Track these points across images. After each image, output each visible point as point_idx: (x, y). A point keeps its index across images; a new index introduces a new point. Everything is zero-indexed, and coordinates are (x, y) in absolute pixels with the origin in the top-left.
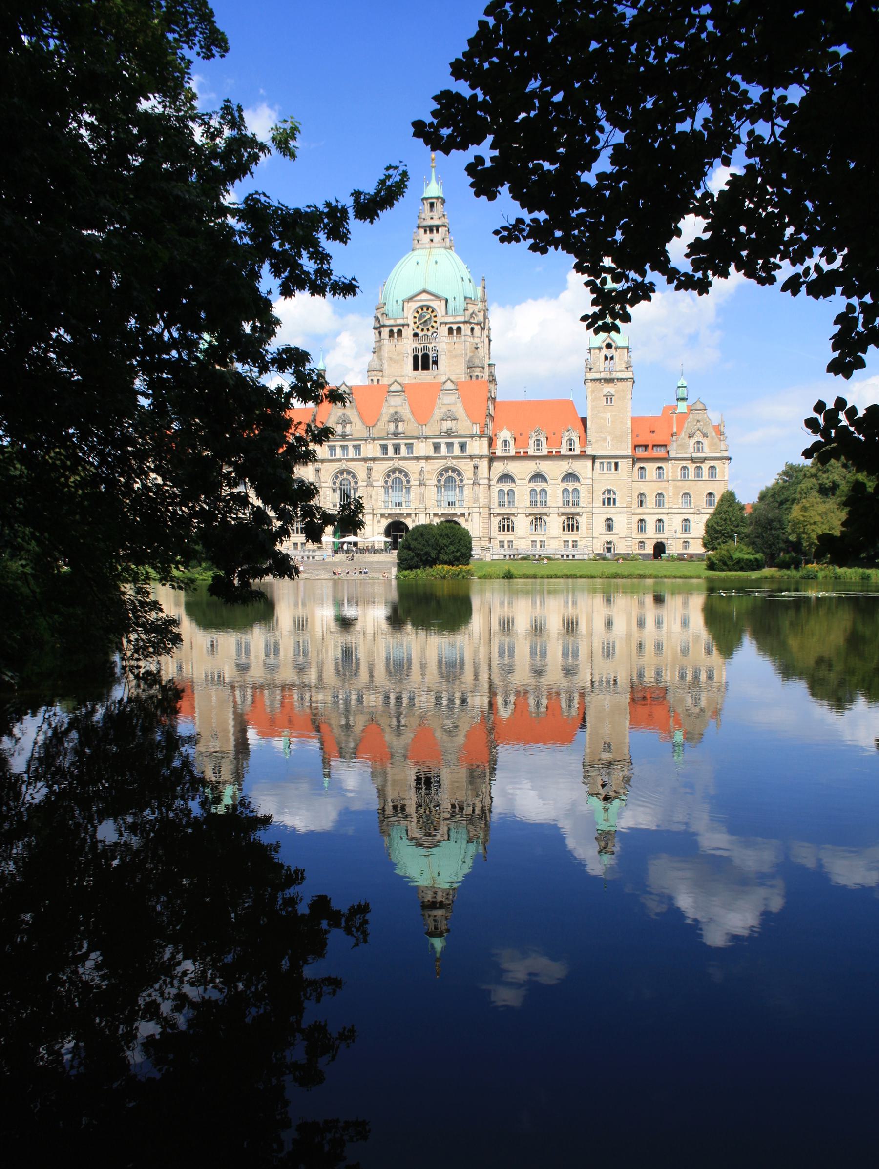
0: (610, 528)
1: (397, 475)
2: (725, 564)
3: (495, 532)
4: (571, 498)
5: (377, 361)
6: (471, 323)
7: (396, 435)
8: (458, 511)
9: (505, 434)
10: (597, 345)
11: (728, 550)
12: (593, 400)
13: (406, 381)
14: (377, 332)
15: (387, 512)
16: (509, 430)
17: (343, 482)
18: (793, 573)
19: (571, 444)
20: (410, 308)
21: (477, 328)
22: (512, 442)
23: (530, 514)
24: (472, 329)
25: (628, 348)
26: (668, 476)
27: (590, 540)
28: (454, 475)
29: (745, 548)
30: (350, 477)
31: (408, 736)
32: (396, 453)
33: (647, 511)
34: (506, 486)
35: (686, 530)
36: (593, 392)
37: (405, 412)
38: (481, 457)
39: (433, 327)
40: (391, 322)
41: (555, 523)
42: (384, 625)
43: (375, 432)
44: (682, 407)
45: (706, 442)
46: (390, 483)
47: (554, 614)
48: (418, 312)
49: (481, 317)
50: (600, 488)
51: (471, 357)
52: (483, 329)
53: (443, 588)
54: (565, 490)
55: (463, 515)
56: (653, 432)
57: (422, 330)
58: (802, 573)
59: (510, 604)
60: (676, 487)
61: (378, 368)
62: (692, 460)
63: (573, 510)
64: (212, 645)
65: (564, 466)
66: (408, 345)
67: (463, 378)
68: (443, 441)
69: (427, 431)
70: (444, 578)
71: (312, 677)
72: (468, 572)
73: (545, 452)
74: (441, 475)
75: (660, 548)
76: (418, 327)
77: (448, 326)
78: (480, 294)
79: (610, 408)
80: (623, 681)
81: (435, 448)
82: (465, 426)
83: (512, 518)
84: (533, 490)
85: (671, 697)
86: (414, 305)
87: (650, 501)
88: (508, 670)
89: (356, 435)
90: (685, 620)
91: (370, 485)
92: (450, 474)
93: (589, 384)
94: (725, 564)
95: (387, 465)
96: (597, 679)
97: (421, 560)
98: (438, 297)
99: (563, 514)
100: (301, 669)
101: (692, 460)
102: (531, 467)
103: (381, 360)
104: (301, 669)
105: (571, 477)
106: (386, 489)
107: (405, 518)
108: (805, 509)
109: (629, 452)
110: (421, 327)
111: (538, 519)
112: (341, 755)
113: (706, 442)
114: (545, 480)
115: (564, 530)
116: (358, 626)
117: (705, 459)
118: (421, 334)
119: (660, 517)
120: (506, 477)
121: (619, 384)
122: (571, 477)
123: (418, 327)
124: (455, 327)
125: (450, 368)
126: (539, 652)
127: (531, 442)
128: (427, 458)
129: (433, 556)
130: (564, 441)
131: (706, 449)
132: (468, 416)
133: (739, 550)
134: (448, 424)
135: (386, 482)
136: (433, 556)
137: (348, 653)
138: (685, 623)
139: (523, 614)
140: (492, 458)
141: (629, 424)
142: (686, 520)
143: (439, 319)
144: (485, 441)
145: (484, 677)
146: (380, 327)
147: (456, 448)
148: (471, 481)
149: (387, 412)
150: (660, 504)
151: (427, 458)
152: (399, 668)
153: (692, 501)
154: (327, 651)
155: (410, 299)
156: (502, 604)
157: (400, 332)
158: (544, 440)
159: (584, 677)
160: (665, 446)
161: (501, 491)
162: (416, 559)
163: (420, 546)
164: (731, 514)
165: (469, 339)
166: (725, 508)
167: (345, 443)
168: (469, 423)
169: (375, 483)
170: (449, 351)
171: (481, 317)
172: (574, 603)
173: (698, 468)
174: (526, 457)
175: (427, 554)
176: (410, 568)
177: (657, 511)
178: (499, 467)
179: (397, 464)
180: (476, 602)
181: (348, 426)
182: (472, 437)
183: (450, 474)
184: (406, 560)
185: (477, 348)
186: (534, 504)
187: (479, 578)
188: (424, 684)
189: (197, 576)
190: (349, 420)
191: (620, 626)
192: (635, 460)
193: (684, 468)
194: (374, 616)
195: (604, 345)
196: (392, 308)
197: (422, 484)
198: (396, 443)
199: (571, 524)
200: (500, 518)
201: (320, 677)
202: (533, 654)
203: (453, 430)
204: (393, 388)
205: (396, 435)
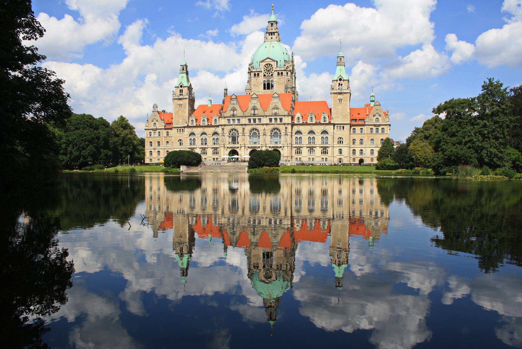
1: (255, 131)
2: (383, 167)
3: (294, 154)
4: (325, 140)
5: (249, 86)
7: (254, 115)
8: (279, 145)
9: (298, 115)
10: (336, 79)
11: (384, 162)
12: (334, 101)
13: (261, 93)
15: (250, 146)
16: (300, 113)
18: (410, 171)
21: (289, 73)
22: (301, 118)
23: (308, 147)
24: (287, 73)
25: (348, 80)
27: (333, 157)
28: (278, 131)
29: (391, 161)
30: (235, 132)
31: (258, 237)
34: (298, 136)
35: (370, 155)
36: (334, 98)
37: (258, 106)
38: (288, 124)
40: (255, 70)
41: (318, 151)
43: (246, 114)
44: (372, 104)
45: (380, 118)
47: (317, 188)
49: (291, 68)
50: (336, 137)
52: (292, 73)
53: (266, 177)
54: (322, 137)
55: (281, 147)
58: (413, 171)
59: (300, 184)
60: (368, 136)
62: (375, 125)
63: (325, 146)
65: (322, 128)
66: (261, 79)
67: (283, 92)
68: (273, 118)
69: (267, 113)
70: (267, 172)
71: (219, 212)
73: (314, 122)
74: (272, 131)
75: (361, 161)
78: (291, 59)
82: (282, 111)
84: (309, 137)
85: (366, 222)
86: (264, 64)
87: (358, 142)
88: (298, 211)
90: (370, 191)
92: (276, 131)
93: (333, 95)
94: (383, 167)
95: (250, 127)
96: (335, 214)
98: (274, 61)
99: (321, 147)
100: (215, 209)
101: (375, 125)
102: (308, 128)
104: (215, 209)
105: (325, 132)
106: (250, 137)
108: (415, 145)
111: (311, 149)
112: (231, 245)
113: (380, 118)
116: (239, 192)
117: (380, 125)
118: (267, 75)
119: (361, 149)
120: (299, 132)
122: (325, 132)
124: (280, 72)
125: (278, 88)
126: (311, 203)
127: (309, 118)
128: (267, 124)
130: (322, 118)
131: (380, 121)
132: (283, 107)
133: (389, 161)
135: (250, 134)
137: (234, 203)
138: (372, 192)
139: (305, 187)
140: (293, 125)
141: (349, 111)
142: (372, 150)
143: (274, 69)
144: (290, 118)
145: (289, 214)
147: (278, 120)
149: (251, 106)
150: (361, 143)
151: (267, 124)
152: (254, 209)
155: (263, 61)
156: (297, 184)
157: (258, 74)
158: (314, 117)
159: (329, 214)
160: (364, 120)
161: (296, 138)
166: (386, 145)
168: (283, 110)
171: (291, 68)
172: (326, 184)
174: (307, 124)
176: (253, 168)
178: (296, 128)
179: (254, 126)
180: (282, 182)
182: (285, 116)
183: (276, 131)
186: (310, 143)
187: (281, 172)
188: (264, 216)
191: (345, 193)
192: (351, 126)
193: (371, 129)
194: (245, 187)
196: (255, 65)
197: (265, 135)
198: (254, 118)
199: (325, 151)
200: (296, 149)
201: (223, 212)
202: (309, 204)
204: (253, 96)
205: (254, 115)
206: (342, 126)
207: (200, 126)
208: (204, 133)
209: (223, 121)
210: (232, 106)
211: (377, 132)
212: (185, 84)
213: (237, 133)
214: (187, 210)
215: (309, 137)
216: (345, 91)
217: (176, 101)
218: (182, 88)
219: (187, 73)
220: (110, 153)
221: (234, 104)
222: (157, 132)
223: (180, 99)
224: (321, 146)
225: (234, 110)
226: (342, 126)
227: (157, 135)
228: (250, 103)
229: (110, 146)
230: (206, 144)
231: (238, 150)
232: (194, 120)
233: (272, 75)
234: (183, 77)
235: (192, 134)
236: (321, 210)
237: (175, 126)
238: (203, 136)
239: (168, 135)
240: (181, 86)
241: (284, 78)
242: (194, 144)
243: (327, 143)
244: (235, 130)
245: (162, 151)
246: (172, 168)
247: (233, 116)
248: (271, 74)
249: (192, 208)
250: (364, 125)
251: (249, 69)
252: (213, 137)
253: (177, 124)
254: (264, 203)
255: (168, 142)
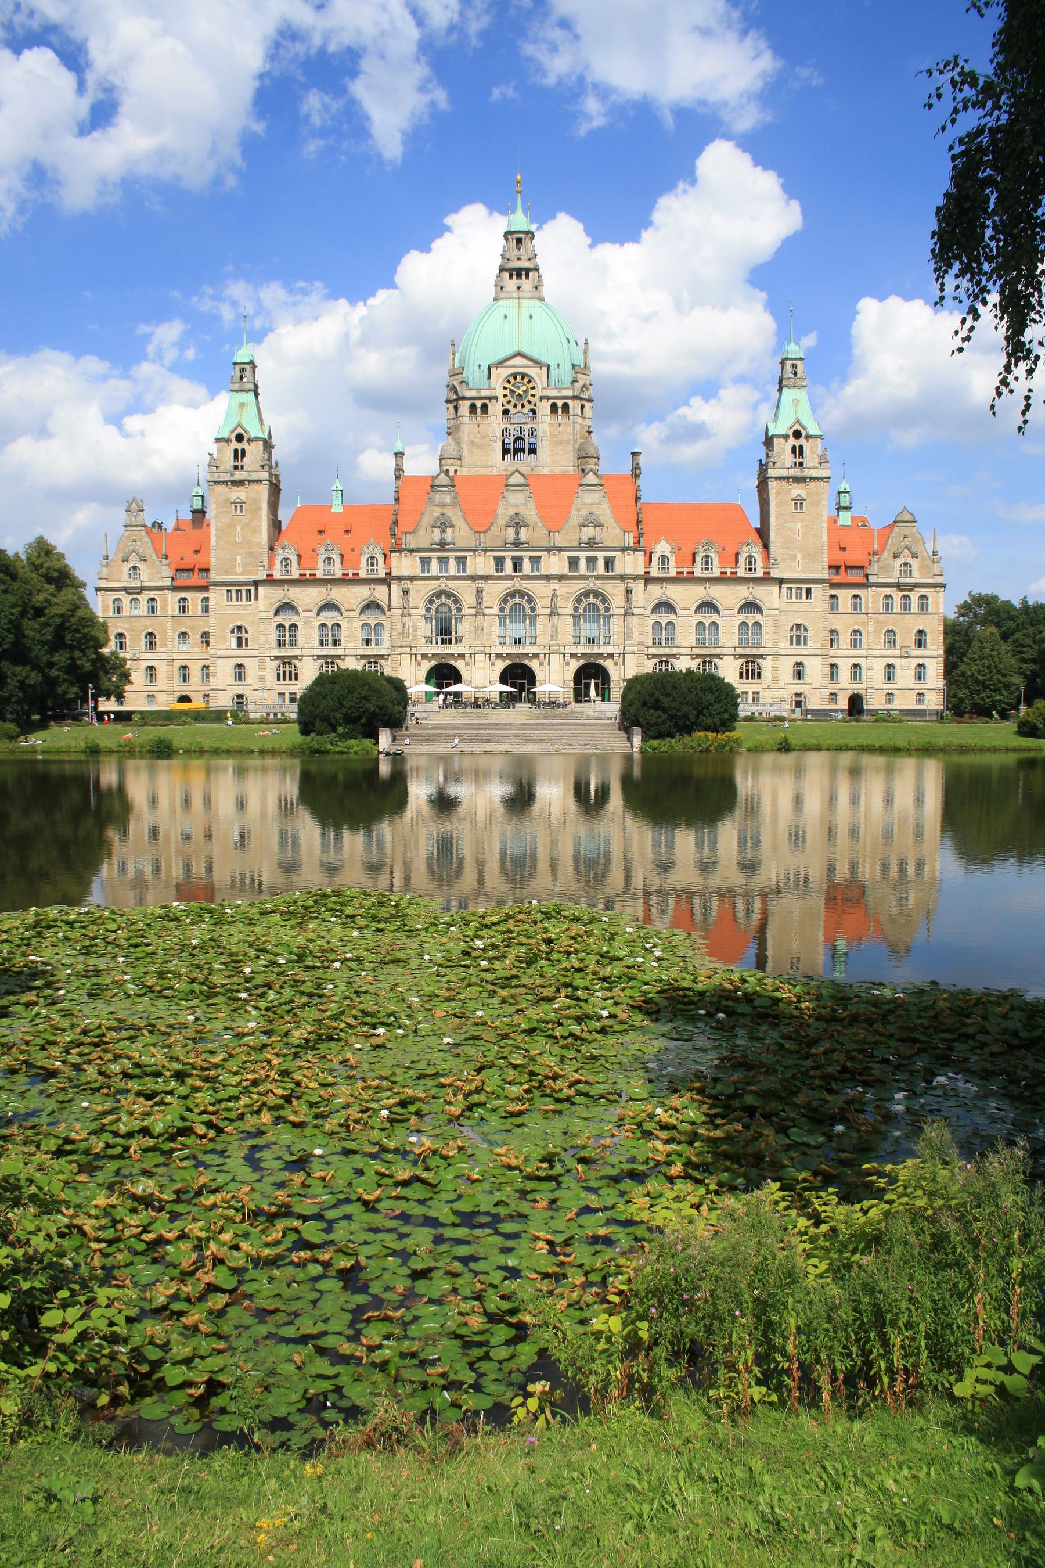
0: (799, 675)
1: (517, 600)
6: (581, 399)
7: (517, 544)
8: (605, 650)
9: (662, 548)
10: (783, 432)
12: (778, 506)
13: (495, 472)
14: (451, 406)
15: (505, 650)
17: (444, 609)
19: (750, 563)
20: (499, 376)
22: (672, 560)
24: (582, 407)
26: (866, 607)
28: (598, 602)
30: (450, 602)
32: (515, 570)
33: (840, 653)
36: (778, 494)
37: (530, 513)
38: (636, 578)
39: (529, 402)
42: (500, 810)
43: (486, 541)
46: (507, 611)
48: (509, 382)
51: (582, 444)
54: (744, 624)
56: (844, 549)
57: (515, 406)
60: (877, 622)
61: (455, 454)
62: (899, 587)
63: (754, 651)
64: (242, 836)
65: (742, 593)
66: (495, 423)
67: (571, 470)
68: (582, 555)
69: (559, 540)
70: (707, 750)
72: (737, 741)
73: (716, 573)
75: (856, 704)
76: (509, 402)
77: (551, 401)
79: (800, 516)
80: (817, 875)
81: (497, 564)
82: (612, 534)
83: (673, 660)
84: (700, 623)
85: (870, 897)
86: (505, 372)
87: (845, 639)
89: (460, 544)
91: (479, 613)
92: (592, 599)
97: (676, 725)
98: (537, 363)
99: (741, 656)
101: (899, 587)
102: (697, 593)
103: (458, 443)
105: (751, 606)
106: (502, 620)
107: (530, 659)
109: (825, 575)
110: (514, 402)
113: (915, 564)
114: (716, 610)
115: (741, 677)
116: (463, 809)
117: (913, 587)
118: (513, 411)
120: (665, 606)
121: (812, 484)
122: (751, 606)
123: (509, 402)
125: (553, 459)
128: (561, 578)
129: (692, 718)
134: (588, 532)
136: (692, 718)
137: (445, 846)
138: (888, 800)
141: (825, 537)
142: (889, 665)
143: (538, 392)
144: (640, 557)
146: (457, 400)
147: (601, 563)
148: (622, 611)
149: (503, 513)
150: (855, 643)
151: (561, 578)
153: (898, 640)
154: (416, 842)
155: (500, 364)
157: (485, 407)
159: (769, 874)
162: (669, 723)
163: (674, 704)
164: (996, 659)
165: (579, 420)
167: (445, 554)
168: (618, 531)
169: (486, 611)
170: (553, 436)
173: (905, 597)
174: (692, 579)
175: (685, 716)
176: (659, 736)
177: (853, 653)
178: (656, 592)
179: (518, 584)
181: (449, 530)
182: (623, 550)
183: (592, 599)
184: (656, 724)
185: (590, 433)
187: (749, 750)
189: (329, 746)
190: (450, 522)
191: (814, 804)
193: (888, 597)
195: (791, 432)
196: (474, 375)
198: (516, 555)
200: (655, 661)
201: (407, 879)
203: (597, 540)
205: (517, 544)
206: (804, 588)
207: (314, 581)
208: (329, 606)
209: (405, 565)
210: (437, 512)
211: (906, 606)
212: (254, 431)
213: (453, 607)
214: (269, 875)
215: (700, 623)
216: (814, 473)
217: (220, 489)
218: (244, 445)
219: (257, 395)
220: (35, 678)
221: (444, 505)
222: (144, 598)
223: (241, 483)
224: (740, 651)
225: (444, 524)
226: (805, 586)
227: (143, 609)
228: (502, 501)
229: (30, 649)
230: (336, 643)
231: (460, 665)
232: (294, 560)
233: (534, 412)
234: (242, 405)
235: (287, 607)
236: (696, 861)
237: (219, 578)
238: (326, 614)
239: (184, 609)
240: (240, 438)
241: (570, 428)
242: (292, 643)
243: (759, 645)
244: (449, 595)
245: (162, 668)
246: (343, 737)
247: (443, 545)
248: (528, 407)
249: (289, 868)
250: (865, 586)
251: (454, 389)
252: (365, 618)
253: (226, 573)
254: (554, 843)
255: (184, 635)
